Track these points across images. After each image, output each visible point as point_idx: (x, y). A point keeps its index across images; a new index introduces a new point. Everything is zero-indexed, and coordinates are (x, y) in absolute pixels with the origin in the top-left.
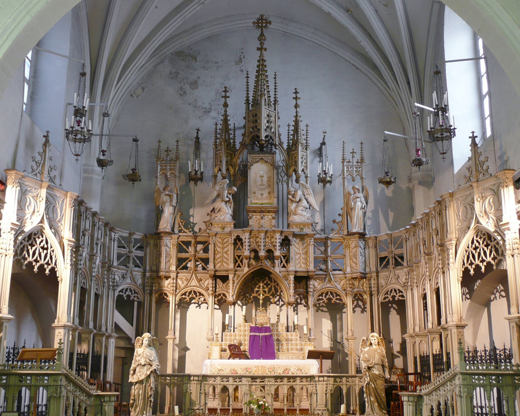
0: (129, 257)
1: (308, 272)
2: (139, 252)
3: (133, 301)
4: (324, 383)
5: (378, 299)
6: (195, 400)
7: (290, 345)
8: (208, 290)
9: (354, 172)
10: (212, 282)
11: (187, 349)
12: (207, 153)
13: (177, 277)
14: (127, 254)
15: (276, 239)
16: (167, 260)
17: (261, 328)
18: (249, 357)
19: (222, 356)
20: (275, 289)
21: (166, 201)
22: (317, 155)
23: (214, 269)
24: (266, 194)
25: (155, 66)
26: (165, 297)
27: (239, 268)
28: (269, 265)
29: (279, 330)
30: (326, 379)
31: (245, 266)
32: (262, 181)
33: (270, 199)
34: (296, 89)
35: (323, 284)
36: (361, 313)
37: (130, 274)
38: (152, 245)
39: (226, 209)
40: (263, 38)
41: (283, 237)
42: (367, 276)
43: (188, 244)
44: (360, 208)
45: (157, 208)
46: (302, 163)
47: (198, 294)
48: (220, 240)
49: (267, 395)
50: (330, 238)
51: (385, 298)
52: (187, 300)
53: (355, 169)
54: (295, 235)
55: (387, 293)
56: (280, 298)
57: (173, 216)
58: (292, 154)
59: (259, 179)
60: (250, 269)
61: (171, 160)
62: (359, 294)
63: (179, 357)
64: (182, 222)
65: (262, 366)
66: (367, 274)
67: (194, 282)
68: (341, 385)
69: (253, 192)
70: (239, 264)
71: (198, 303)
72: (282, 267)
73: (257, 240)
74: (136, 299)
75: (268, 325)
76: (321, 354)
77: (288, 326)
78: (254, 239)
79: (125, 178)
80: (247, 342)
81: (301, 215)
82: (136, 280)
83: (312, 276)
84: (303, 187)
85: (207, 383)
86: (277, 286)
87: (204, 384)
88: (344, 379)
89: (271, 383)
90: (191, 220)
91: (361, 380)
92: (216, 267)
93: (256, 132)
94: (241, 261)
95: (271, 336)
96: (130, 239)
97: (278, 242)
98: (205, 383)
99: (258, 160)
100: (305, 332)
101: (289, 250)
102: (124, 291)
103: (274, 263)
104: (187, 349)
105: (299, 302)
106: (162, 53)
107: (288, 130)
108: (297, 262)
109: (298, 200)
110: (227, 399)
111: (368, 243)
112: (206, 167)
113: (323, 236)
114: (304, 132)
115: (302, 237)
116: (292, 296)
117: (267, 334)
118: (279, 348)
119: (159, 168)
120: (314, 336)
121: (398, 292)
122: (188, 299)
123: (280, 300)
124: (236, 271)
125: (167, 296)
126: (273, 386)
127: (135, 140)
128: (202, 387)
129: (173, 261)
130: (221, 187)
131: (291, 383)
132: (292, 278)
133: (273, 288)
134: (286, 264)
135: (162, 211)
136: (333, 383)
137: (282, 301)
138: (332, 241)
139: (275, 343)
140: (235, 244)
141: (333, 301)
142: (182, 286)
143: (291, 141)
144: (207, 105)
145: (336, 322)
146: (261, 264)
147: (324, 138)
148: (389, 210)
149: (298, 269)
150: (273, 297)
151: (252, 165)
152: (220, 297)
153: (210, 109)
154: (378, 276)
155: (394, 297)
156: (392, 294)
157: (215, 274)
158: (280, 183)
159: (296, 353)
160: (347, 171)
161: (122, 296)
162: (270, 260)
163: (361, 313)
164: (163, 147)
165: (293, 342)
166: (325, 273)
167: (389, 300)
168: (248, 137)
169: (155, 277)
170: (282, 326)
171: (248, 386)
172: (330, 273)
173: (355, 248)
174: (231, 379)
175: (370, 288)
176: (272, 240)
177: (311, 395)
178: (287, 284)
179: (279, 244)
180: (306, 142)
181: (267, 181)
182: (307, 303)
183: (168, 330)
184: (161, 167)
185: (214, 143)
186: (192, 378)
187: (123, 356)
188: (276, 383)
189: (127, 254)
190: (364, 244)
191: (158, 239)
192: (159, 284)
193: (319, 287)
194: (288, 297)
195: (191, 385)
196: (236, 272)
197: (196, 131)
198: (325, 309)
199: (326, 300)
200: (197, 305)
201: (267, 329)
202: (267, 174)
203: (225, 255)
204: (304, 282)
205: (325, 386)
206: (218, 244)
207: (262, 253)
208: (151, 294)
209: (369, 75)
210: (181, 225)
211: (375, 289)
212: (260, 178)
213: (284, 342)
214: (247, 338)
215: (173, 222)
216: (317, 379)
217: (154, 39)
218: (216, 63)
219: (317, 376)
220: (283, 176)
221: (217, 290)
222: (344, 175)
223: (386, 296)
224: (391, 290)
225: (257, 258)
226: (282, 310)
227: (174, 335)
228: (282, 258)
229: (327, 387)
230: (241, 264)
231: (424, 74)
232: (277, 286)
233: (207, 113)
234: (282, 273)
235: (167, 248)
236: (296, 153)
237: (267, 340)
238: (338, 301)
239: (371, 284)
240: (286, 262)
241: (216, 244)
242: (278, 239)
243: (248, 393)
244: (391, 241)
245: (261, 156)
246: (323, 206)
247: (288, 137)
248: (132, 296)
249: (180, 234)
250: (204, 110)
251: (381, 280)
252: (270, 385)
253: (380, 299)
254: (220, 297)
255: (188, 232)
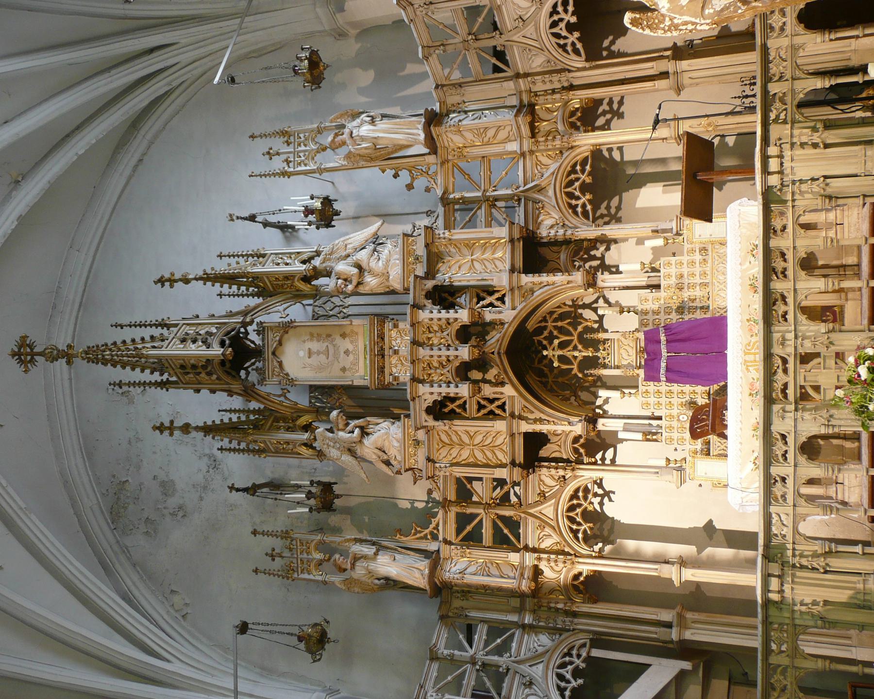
0: (484, 665)
1: (512, 241)
2: (476, 637)
3: (589, 659)
4: (787, 153)
5: (579, 70)
6: (850, 592)
7: (692, 281)
8: (564, 477)
9: (308, 148)
10: (545, 469)
11: (709, 527)
12: (289, 466)
13: (535, 550)
14: (478, 670)
15: (432, 319)
16: (497, 573)
17: (648, 354)
18: (722, 383)
19: (721, 452)
20: (562, 321)
21: (367, 569)
22: (295, 233)
23: (508, 467)
24: (346, 344)
25: (134, 565)
26: (582, 579)
27: (507, 407)
28: (498, 335)
29: (655, 307)
30: (772, 150)
31: (502, 393)
32: (319, 353)
33: (357, 334)
34: (156, 283)
35: (547, 205)
36: (623, 118)
37: (521, 666)
38: (464, 603)
39: (379, 433)
40: (47, 351)
41: (428, 303)
42: (526, 101)
43: (463, 520)
44: (371, 127)
45: (382, 588)
46: (287, 264)
47: (575, 502)
48: (444, 451)
49: (832, 348)
50: (444, 193)
51: (576, 52)
52: (591, 528)
53: (303, 148)
54: (430, 274)
55: (563, 47)
56: (585, 306)
57: (400, 553)
58: (273, 287)
59: (315, 360)
60: (506, 380)
61: (291, 550)
62: (570, 117)
63: (730, 546)
64: (417, 532)
65: (746, 354)
66: (521, 101)
67: (547, 509)
68: (793, 98)
69: (341, 374)
70: (498, 407)
71: (602, 496)
72: (504, 303)
73: (436, 364)
74: (584, 654)
75: (641, 336)
76: (695, 176)
77: (648, 287)
78: (432, 371)
79: (318, 657)
80: (687, 388)
81: (388, 261)
82: (540, 650)
83: (521, 231)
84: (329, 260)
85: (790, 546)
86: (555, 316)
87: (794, 555)
88: (774, 88)
89: (791, 336)
90: (421, 505)
91: (777, 28)
92: (504, 461)
93: (213, 367)
94: (491, 401)
95: (667, 328)
96: (445, 659)
97: (439, 316)
98: (789, 553)
99: (275, 363)
100: (659, 242)
101: (462, 289)
102: (563, 684)
103: (493, 324)
104: (709, 527)
105: (598, 262)
106: (110, 551)
107: (229, 296)
108: (490, 267)
109: (355, 271)
110: (835, 442)
111: (453, 105)
112: (315, 469)
113: (440, 210)
114: (233, 261)
115: (434, 259)
116: (570, 278)
117: (663, 338)
118: (702, 308)
119: (306, 576)
120: (671, 221)
121: (556, 18)
122: (585, 526)
123: (595, 305)
124: (512, 415)
125: (580, 574)
126: (801, 328)
127: (243, 628)
128: (804, 562)
129: (498, 556)
130: (332, 444)
131: (790, 265)
132: (527, 280)
133: (559, 324)
134: (497, 295)
135: (387, 579)
136: (788, 126)
137: (596, 301)
138: (451, 189)
139: (687, 317)
140: (452, 415)
141: (588, 180)
142: (556, 538)
143: (251, 289)
144: (203, 464)
145: (647, 173)
146: (496, 353)
147: (242, 218)
148: (401, 74)
149: (508, 266)
150: (581, 323)
151: (287, 374)
152: (582, 451)
153: (210, 457)
154: (526, 75)
155: (570, 28)
156: (564, 33)
157: (520, 465)
158: (344, 311)
159: (713, 263)
160: (305, 165)
161: (573, 690)
162: (488, 333)
163: (623, 118)
164: (267, 564)
165: (685, 270)
166: (523, 200)
167: (578, 39)
168: (228, 384)
169: (536, 600)
170: (646, 300)
171: (799, 414)
172: (521, 189)
173: (464, 133)
174: (775, 471)
175: (554, 91)
176: (436, 328)
177: (830, 197)
178: (541, 291)
179: (443, 311)
180: (250, 258)
181: (318, 341)
182: (594, 243)
183: (659, 577)
184: (305, 571)
185: (257, 456)
186: (774, 597)
187: (726, 683)
188: (791, 317)
189: (478, 670)
190: (454, 115)
191: (451, 589)
192: (552, 591)
193: (556, 215)
194: (572, 288)
195: (798, 599)
196: (517, 414)
197: (234, 492)
198: (615, 202)
199: (584, 195)
200: (606, 499)
201: (652, 338)
202: (304, 342)
203: (478, 439)
204: (545, 252)
205: (799, 152)
206: (454, 456)
207: (465, 353)
208: (575, 615)
209: (149, 136)
210: (422, 535)
211: (555, 77)
212: (314, 357)
213: (686, 294)
214: (675, 387)
215: (412, 553)
216: (774, 180)
217: (67, 572)
218: (130, 442)
219: (764, 181)
220: (332, 306)
221: (565, 457)
222: (313, 172)
223: (569, 48)
224: (557, 36)
225: (481, 363)
226: (617, 302)
227: (673, 563)
228: (481, 303)
229: (803, 145)
230: (497, 403)
231: (126, 18)
232: (555, 316)
233: (218, 463)
234: (517, 303)
235: (468, 571)
236: (268, 278)
237: (679, 337)
238: (588, 168)
239: (545, 91)
240: (491, 293)
241: (455, 461)
242: (431, 316)
243: (826, 415)
244: (439, 46)
245: (268, 354)
246: (392, 217)
247: (243, 296)
248: (577, 662)
249: (441, 538)
250: (211, 470)
251: (534, 65)
252: (796, 337)
253: (580, 65)
254: (582, 451)
255: (436, 519)
